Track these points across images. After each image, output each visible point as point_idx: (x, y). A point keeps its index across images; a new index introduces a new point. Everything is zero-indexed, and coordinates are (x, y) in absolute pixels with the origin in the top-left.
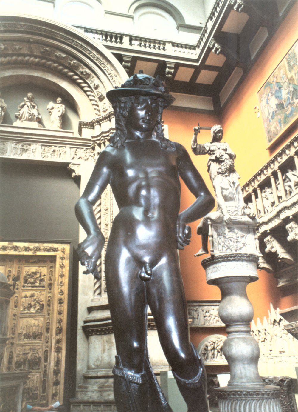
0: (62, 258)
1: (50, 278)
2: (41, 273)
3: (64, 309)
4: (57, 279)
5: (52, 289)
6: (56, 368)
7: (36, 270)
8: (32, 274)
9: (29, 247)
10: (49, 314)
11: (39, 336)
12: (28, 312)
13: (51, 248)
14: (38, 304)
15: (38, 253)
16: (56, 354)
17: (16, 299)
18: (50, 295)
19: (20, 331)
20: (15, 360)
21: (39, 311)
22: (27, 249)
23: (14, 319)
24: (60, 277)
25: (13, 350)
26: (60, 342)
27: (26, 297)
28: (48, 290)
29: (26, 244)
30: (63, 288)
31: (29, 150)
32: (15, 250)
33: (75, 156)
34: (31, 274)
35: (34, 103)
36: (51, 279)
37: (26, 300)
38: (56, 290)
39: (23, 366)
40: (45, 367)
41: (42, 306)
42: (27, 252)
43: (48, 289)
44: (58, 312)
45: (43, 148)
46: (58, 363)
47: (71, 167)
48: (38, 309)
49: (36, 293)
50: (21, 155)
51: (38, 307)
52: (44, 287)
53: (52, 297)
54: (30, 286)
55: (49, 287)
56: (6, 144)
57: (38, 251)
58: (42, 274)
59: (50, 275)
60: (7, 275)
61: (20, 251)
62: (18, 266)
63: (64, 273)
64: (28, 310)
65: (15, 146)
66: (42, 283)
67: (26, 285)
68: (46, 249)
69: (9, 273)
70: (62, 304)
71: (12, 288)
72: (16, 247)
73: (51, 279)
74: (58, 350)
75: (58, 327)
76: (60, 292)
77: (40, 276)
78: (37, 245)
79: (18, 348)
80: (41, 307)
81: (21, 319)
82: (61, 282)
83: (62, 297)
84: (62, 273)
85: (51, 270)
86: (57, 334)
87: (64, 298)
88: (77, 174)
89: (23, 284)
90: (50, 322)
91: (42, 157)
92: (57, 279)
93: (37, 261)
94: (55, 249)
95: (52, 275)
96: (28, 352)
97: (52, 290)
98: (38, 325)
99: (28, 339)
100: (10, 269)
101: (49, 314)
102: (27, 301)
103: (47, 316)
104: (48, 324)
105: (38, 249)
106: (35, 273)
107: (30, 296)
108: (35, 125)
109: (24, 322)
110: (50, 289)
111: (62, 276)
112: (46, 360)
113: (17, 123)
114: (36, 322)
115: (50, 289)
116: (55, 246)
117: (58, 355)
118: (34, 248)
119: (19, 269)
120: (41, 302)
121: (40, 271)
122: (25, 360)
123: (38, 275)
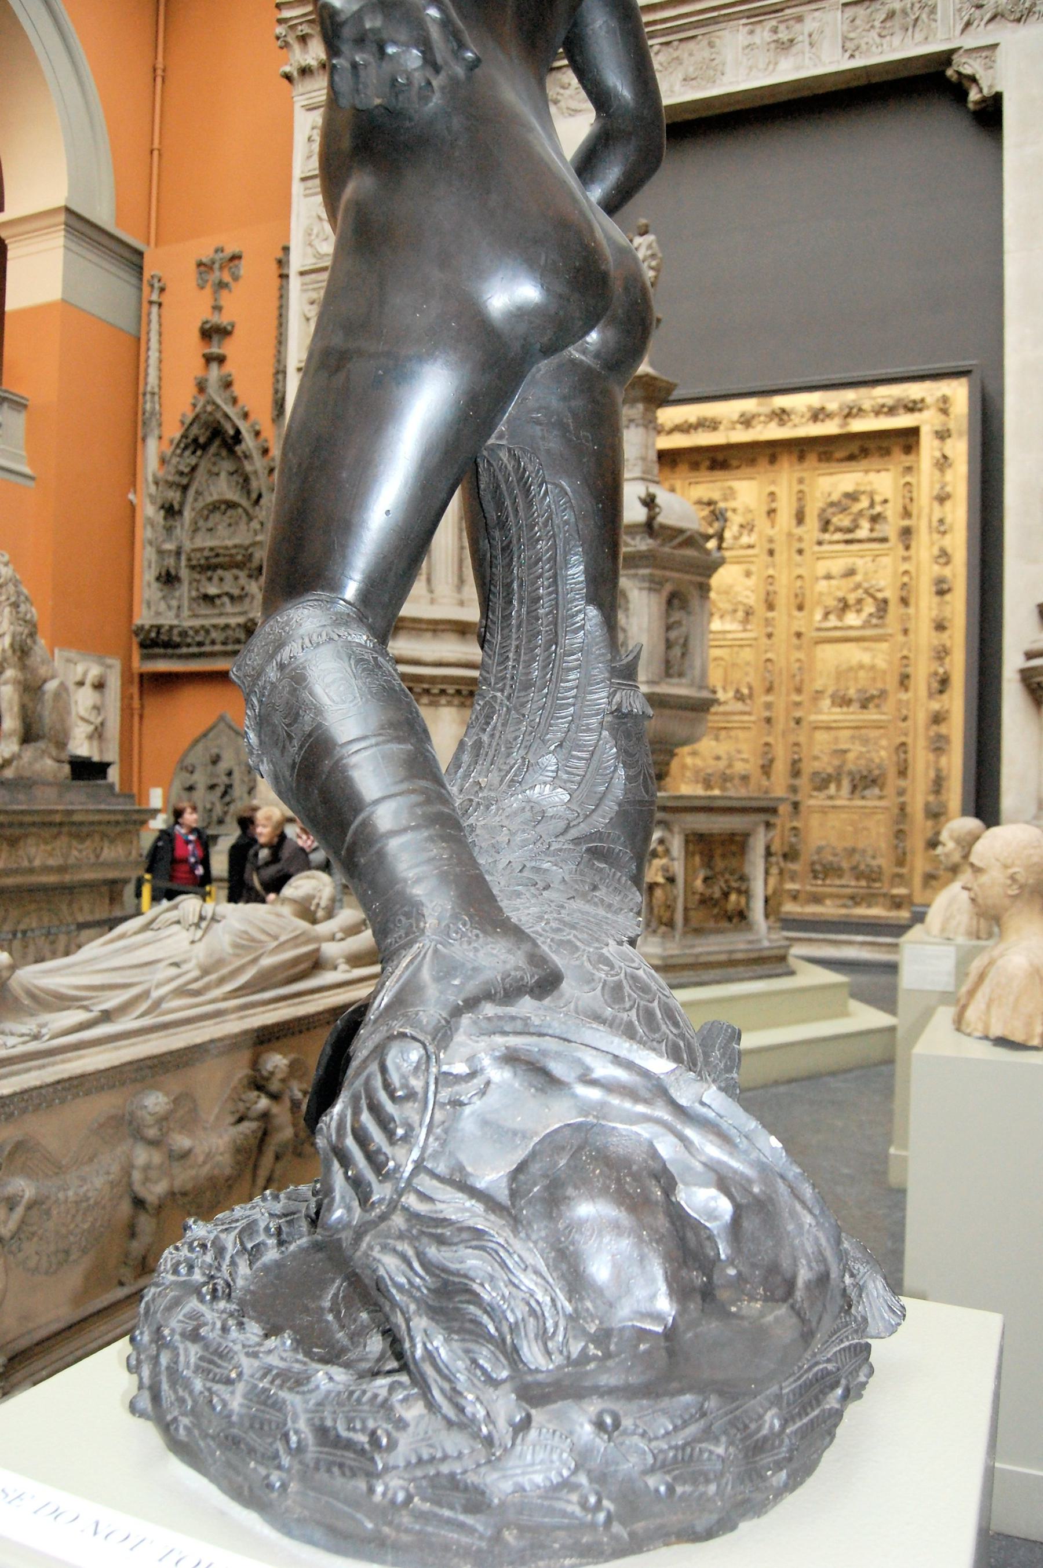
0: (942, 435)
1: (905, 508)
2: (871, 495)
3: (952, 613)
4: (925, 511)
5: (913, 544)
6: (931, 798)
7: (858, 484)
8: (844, 501)
9: (823, 409)
10: (906, 632)
11: (876, 701)
12: (839, 624)
13: (899, 400)
14: (870, 600)
15: (858, 426)
16: (931, 757)
17: (799, 583)
18: (906, 566)
19: (818, 685)
20: (808, 768)
21: (874, 621)
22: (817, 415)
23: (799, 648)
24: (936, 504)
25: (802, 739)
26: (944, 719)
27: (828, 577)
28: (901, 551)
29: (814, 399)
30: (947, 542)
31: (800, 38)
32: (782, 423)
33: (978, 13)
34: (839, 502)
36: (907, 514)
37: (830, 586)
38: (924, 546)
39: (833, 788)
40: (901, 793)
41: (882, 605)
42: (819, 424)
43: (901, 547)
44: (933, 625)
46: (938, 784)
47: (967, 66)
48: (871, 615)
49: (859, 563)
50: (771, 67)
51: (870, 608)
52: (884, 540)
53: (914, 574)
54: (838, 542)
55: (903, 541)
56: (718, 42)
57: (856, 416)
58: (878, 499)
59: (904, 497)
60: (765, 508)
61: (795, 426)
62: (797, 475)
63: (948, 489)
64: (840, 618)
65: (750, 39)
66: (877, 527)
67: (827, 536)
68: (883, 406)
69: (773, 501)
70: (948, 597)
72: (783, 411)
73: (907, 514)
74: (939, 745)
75: (936, 674)
76: (940, 557)
77: (872, 505)
78: (850, 396)
79: (821, 736)
80: (879, 610)
81: (820, 647)
82: (941, 521)
83: (947, 572)
84: (942, 488)
85: (908, 479)
86: (931, 695)
87: (954, 576)
88: (986, 91)
89: (817, 535)
90: (911, 655)
91: (847, 55)
92: (925, 511)
93: (857, 452)
94: (915, 402)
95: (911, 500)
96: (844, 747)
97: (912, 552)
98: (873, 668)
99: (845, 709)
100: (772, 488)
101: (906, 632)
102: (841, 588)
103: (901, 638)
104: (905, 662)
105: (855, 411)
106: (852, 497)
107: (842, 572)
109: (830, 656)
110: (907, 548)
111: (942, 499)
112: (903, 773)
114: (866, 658)
115: (907, 548)
116: (914, 391)
117: (937, 762)
118: (841, 409)
119: (802, 487)
120: (879, 590)
121: (868, 488)
122: (839, 769)
123: (864, 503)
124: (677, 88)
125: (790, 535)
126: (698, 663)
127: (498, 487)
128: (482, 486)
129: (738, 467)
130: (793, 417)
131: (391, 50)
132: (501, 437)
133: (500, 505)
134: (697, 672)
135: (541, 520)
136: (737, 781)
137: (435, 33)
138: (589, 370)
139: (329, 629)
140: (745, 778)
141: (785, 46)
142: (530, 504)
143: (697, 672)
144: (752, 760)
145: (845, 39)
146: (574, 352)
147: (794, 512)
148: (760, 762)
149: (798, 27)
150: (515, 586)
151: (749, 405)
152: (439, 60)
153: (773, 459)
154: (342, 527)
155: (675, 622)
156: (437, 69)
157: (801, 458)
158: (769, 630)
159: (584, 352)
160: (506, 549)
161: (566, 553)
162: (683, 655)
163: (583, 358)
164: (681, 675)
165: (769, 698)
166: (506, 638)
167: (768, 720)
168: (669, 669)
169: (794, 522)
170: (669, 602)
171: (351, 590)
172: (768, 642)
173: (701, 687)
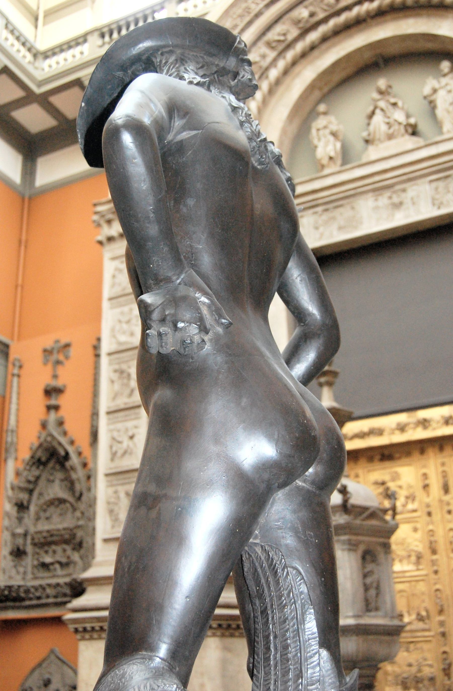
32: (425, 428)
35: (394, 97)
45: (434, 185)
60: (421, 484)
61: (434, 429)
62: (440, 461)
71: (388, 517)
100: (424, 471)
108: (409, 142)
113: (373, 153)
119: (445, 468)
124: (335, 232)
125: (441, 501)
126: (388, 599)
127: (256, 570)
128: (245, 570)
129: (399, 458)
130: (431, 423)
131: (180, 325)
132: (256, 538)
133: (258, 583)
134: (388, 606)
135: (285, 592)
136: (426, 682)
137: (205, 311)
138: (308, 491)
139: (151, 681)
140: (432, 679)
141: (398, 206)
142: (277, 583)
143: (388, 606)
144: (435, 665)
145: (433, 199)
146: (299, 483)
147: (441, 485)
148: (442, 667)
149: (403, 195)
150: (272, 638)
151: (402, 418)
152: (208, 326)
153: (422, 452)
154: (156, 608)
155: (368, 572)
156: (206, 331)
157: (441, 449)
158: (435, 568)
159: (304, 481)
160: (264, 612)
161: (303, 614)
162: (377, 595)
163: (304, 485)
164: (377, 609)
165: (442, 618)
166: (267, 674)
167: (443, 634)
168: (369, 606)
169: (442, 492)
170: (364, 558)
171: (163, 650)
172: (436, 577)
173: (392, 618)
